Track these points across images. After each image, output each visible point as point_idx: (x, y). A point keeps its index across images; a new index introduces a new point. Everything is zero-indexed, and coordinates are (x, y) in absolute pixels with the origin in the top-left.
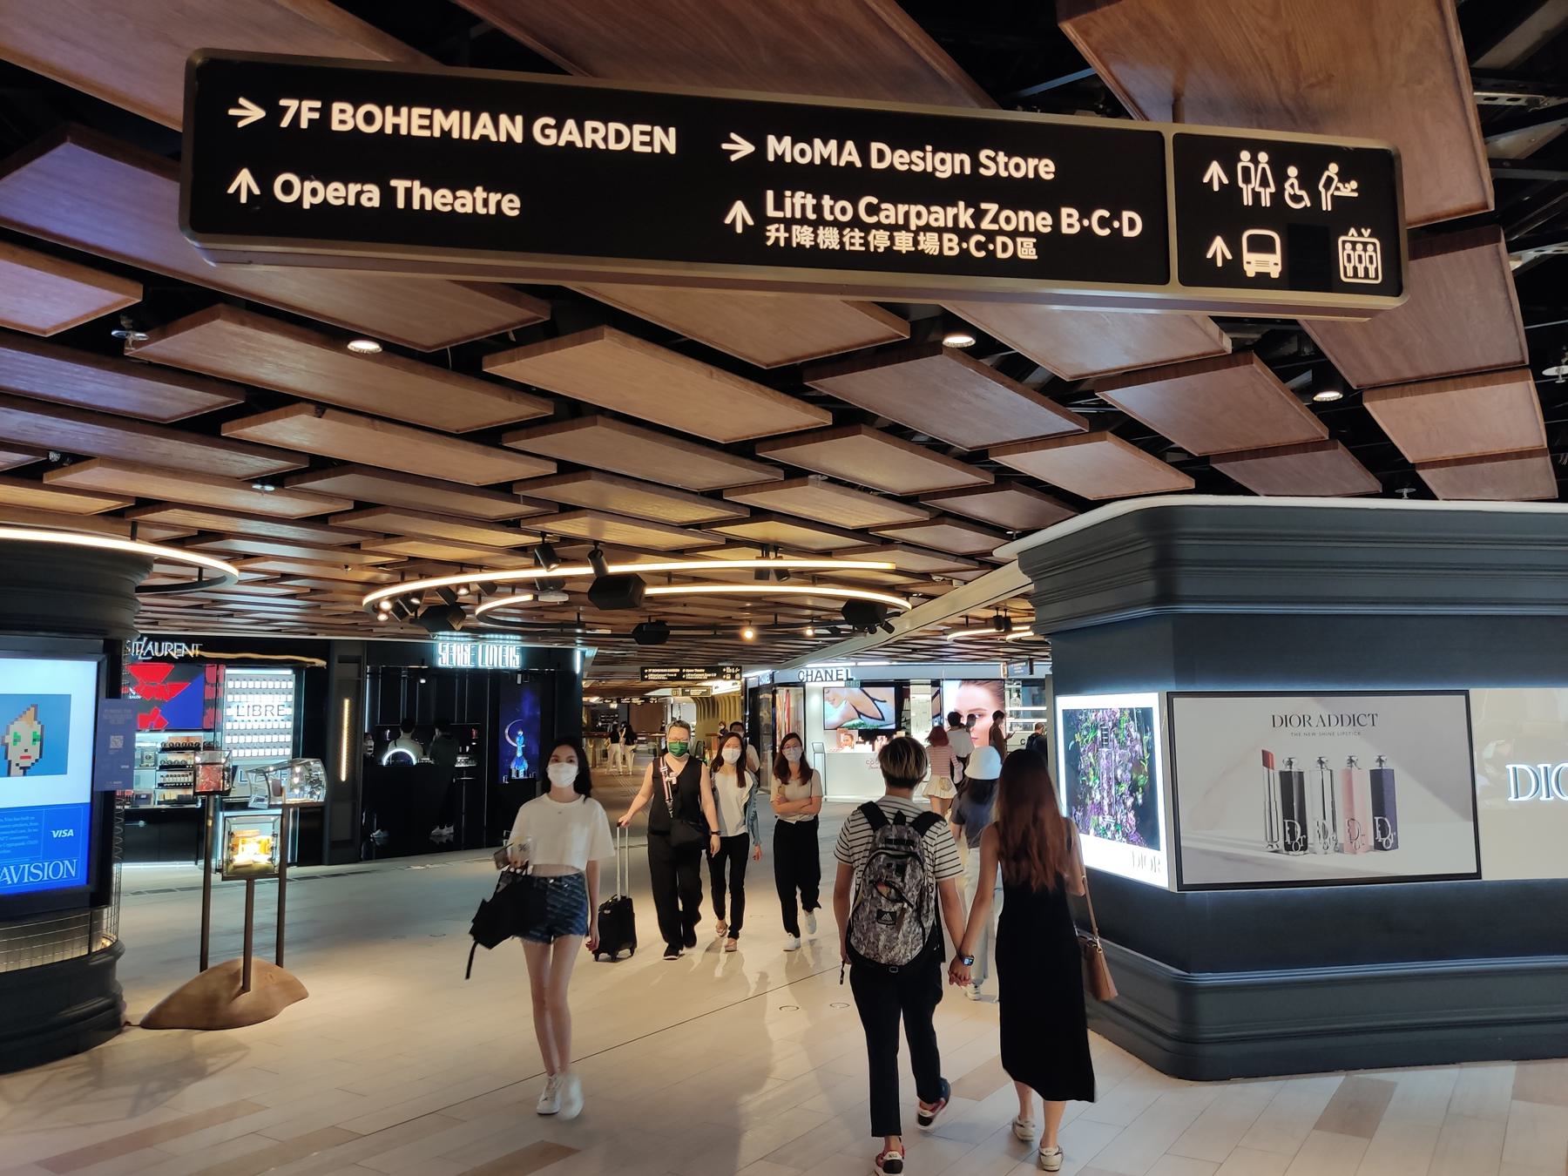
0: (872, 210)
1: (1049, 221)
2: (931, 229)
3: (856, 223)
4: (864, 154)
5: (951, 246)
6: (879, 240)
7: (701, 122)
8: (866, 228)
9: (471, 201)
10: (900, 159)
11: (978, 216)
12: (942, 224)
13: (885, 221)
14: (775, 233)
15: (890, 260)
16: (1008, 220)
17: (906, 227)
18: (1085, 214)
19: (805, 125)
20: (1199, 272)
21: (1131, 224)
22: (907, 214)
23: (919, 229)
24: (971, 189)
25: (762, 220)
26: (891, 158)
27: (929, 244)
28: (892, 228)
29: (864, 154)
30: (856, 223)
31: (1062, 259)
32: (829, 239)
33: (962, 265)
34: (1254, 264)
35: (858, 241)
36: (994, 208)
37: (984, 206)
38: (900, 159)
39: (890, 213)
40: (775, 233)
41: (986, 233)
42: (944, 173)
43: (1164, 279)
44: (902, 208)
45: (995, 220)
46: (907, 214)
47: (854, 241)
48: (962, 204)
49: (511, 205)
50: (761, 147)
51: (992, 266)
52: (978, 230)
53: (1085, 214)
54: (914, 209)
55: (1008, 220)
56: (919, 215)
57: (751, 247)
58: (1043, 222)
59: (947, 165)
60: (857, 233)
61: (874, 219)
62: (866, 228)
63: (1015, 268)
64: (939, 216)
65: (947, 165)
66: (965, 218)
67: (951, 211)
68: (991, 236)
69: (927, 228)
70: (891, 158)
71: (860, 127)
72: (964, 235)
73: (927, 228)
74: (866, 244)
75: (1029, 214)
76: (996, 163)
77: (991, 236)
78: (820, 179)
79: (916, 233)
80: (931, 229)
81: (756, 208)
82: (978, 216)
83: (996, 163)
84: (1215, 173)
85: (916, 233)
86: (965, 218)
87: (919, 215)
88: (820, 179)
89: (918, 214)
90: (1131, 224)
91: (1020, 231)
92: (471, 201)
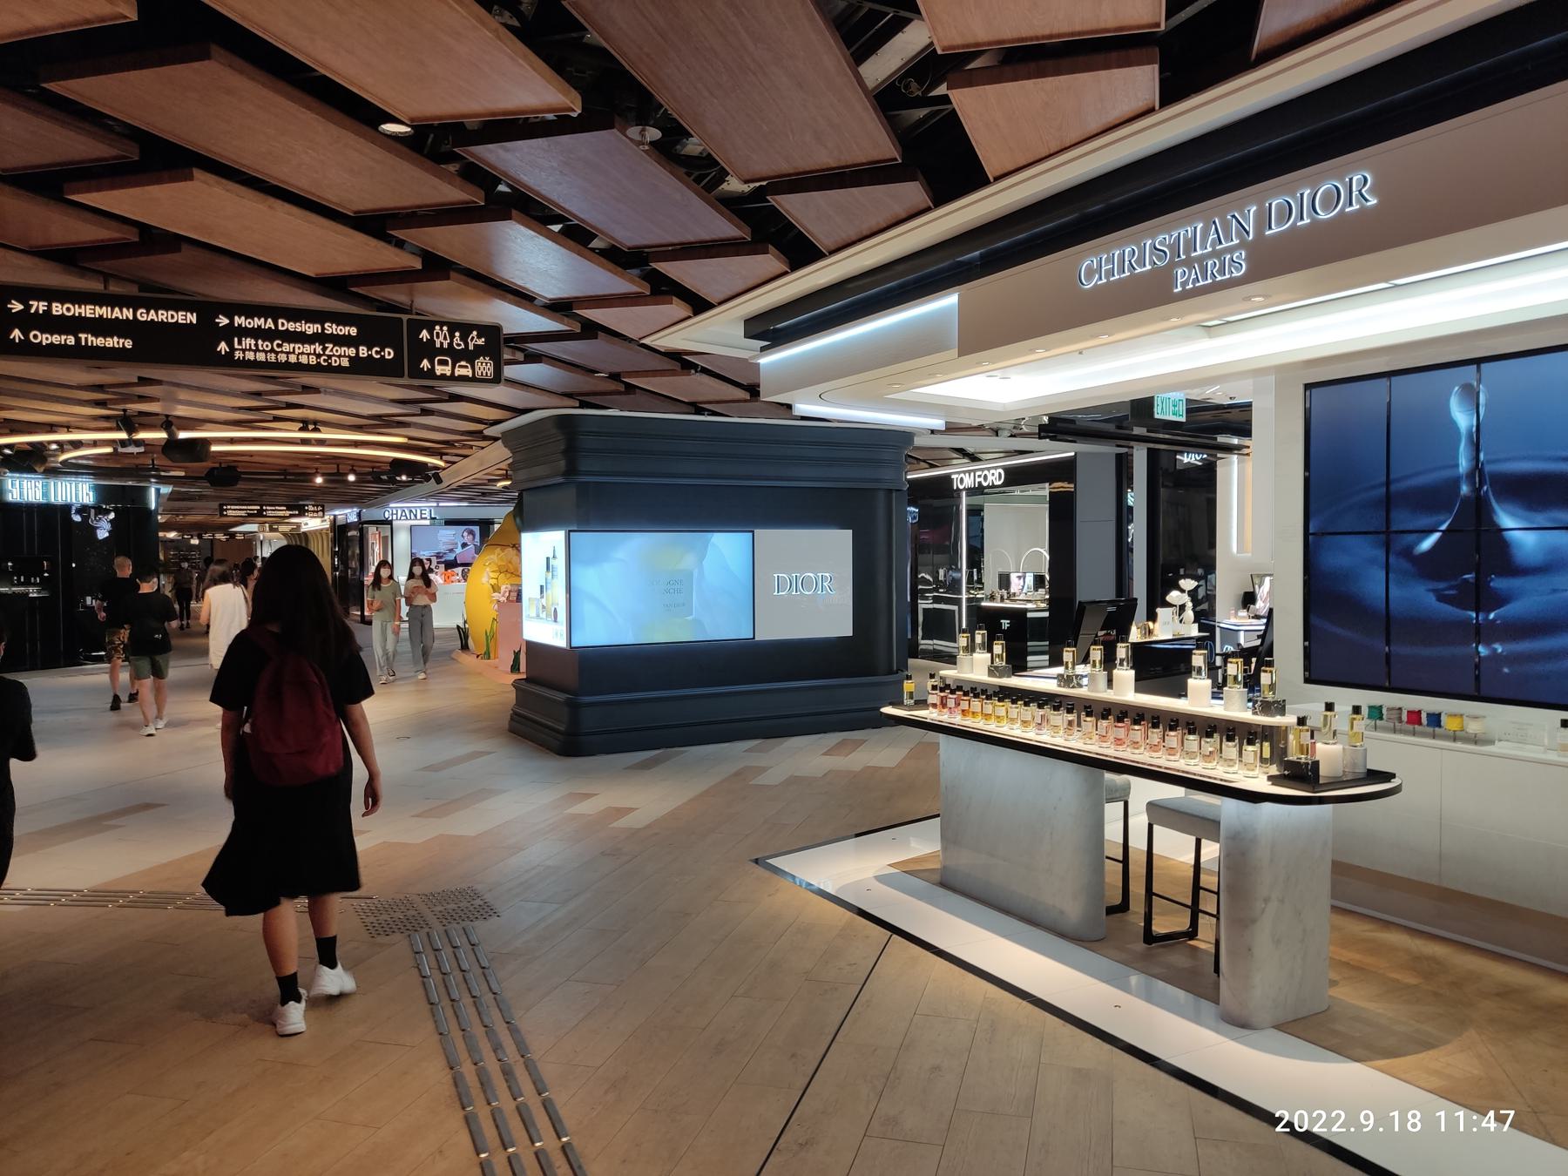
2: (305, 353)
3: (272, 350)
4: (276, 324)
5: (313, 361)
6: (282, 358)
7: (207, 310)
8: (277, 353)
9: (112, 342)
10: (291, 326)
11: (324, 349)
14: (238, 355)
15: (287, 366)
18: (370, 349)
19: (251, 310)
20: (417, 373)
21: (389, 353)
24: (321, 338)
25: (233, 350)
26: (285, 325)
27: (304, 360)
29: (276, 324)
30: (272, 350)
31: (359, 367)
32: (261, 357)
33: (317, 368)
34: (439, 370)
38: (291, 326)
39: (287, 347)
40: (238, 355)
42: (310, 332)
43: (402, 376)
47: (272, 358)
49: (129, 344)
50: (232, 321)
51: (330, 370)
53: (370, 349)
57: (228, 362)
58: (352, 352)
59: (311, 329)
63: (340, 370)
64: (308, 348)
65: (311, 329)
66: (319, 350)
68: (330, 357)
70: (285, 325)
71: (274, 312)
72: (319, 356)
76: (331, 329)
77: (330, 357)
78: (257, 333)
80: (305, 353)
81: (230, 345)
82: (324, 349)
83: (331, 329)
84: (424, 334)
86: (319, 350)
88: (257, 333)
90: (389, 353)
91: (341, 355)
92: (112, 342)
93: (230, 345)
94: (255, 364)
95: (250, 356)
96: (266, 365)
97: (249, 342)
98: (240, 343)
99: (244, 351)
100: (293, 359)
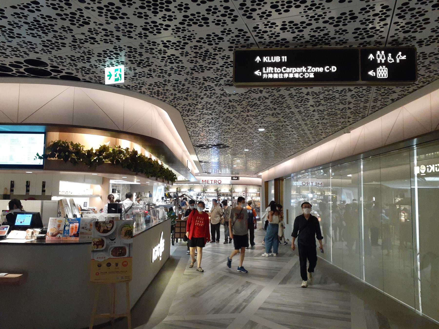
0: (284, 70)
1: (323, 69)
6: (286, 76)
8: (283, 73)
11: (307, 70)
12: (299, 71)
13: (287, 72)
16: (313, 70)
17: (292, 73)
22: (292, 70)
23: (295, 73)
27: (297, 76)
28: (289, 73)
32: (276, 76)
35: (282, 76)
36: (310, 67)
37: (308, 67)
39: (289, 70)
41: (309, 73)
44: (291, 69)
45: (311, 70)
46: (292, 70)
47: (281, 76)
48: (304, 67)
52: (307, 72)
54: (293, 69)
55: (313, 70)
56: (294, 70)
58: (321, 70)
60: (282, 74)
61: (285, 72)
62: (283, 73)
64: (299, 70)
67: (301, 69)
69: (296, 72)
73: (296, 72)
74: (283, 77)
75: (318, 68)
79: (294, 74)
85: (294, 74)
87: (294, 70)
89: (294, 70)
93: (261, 71)
94: (273, 80)
95: (270, 76)
96: (278, 80)
97: (270, 69)
98: (266, 70)
99: (267, 74)
100: (291, 76)
